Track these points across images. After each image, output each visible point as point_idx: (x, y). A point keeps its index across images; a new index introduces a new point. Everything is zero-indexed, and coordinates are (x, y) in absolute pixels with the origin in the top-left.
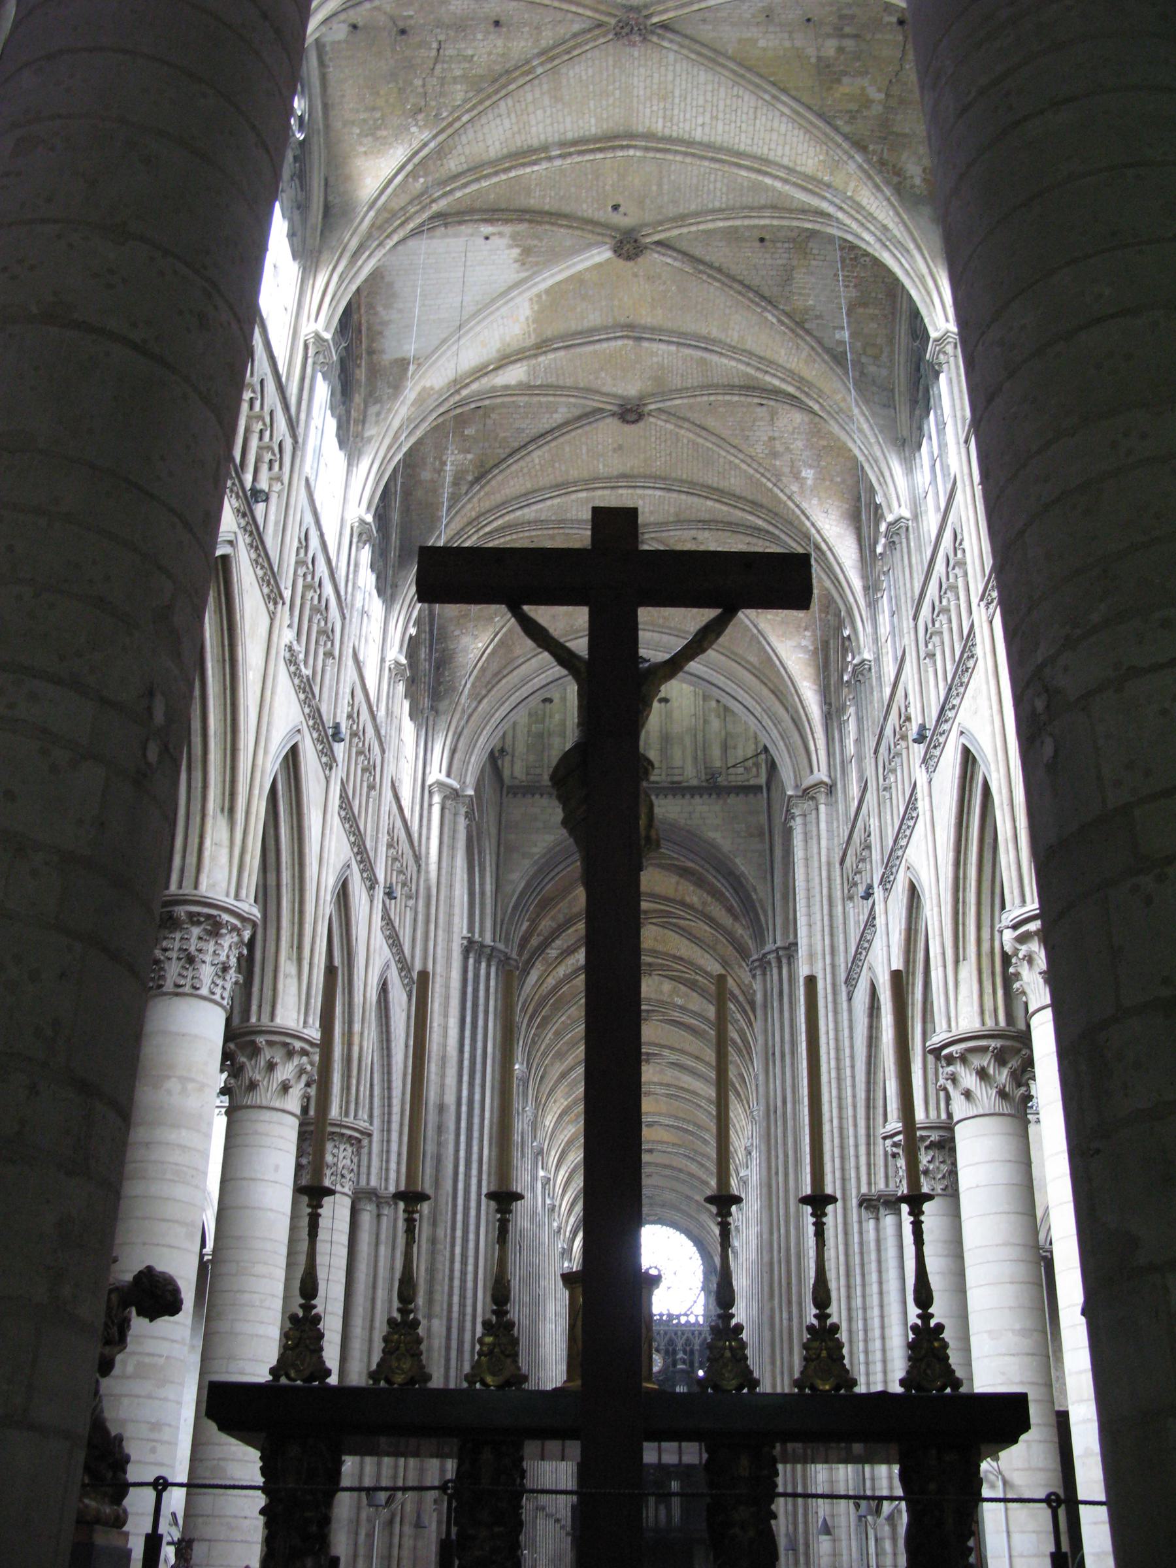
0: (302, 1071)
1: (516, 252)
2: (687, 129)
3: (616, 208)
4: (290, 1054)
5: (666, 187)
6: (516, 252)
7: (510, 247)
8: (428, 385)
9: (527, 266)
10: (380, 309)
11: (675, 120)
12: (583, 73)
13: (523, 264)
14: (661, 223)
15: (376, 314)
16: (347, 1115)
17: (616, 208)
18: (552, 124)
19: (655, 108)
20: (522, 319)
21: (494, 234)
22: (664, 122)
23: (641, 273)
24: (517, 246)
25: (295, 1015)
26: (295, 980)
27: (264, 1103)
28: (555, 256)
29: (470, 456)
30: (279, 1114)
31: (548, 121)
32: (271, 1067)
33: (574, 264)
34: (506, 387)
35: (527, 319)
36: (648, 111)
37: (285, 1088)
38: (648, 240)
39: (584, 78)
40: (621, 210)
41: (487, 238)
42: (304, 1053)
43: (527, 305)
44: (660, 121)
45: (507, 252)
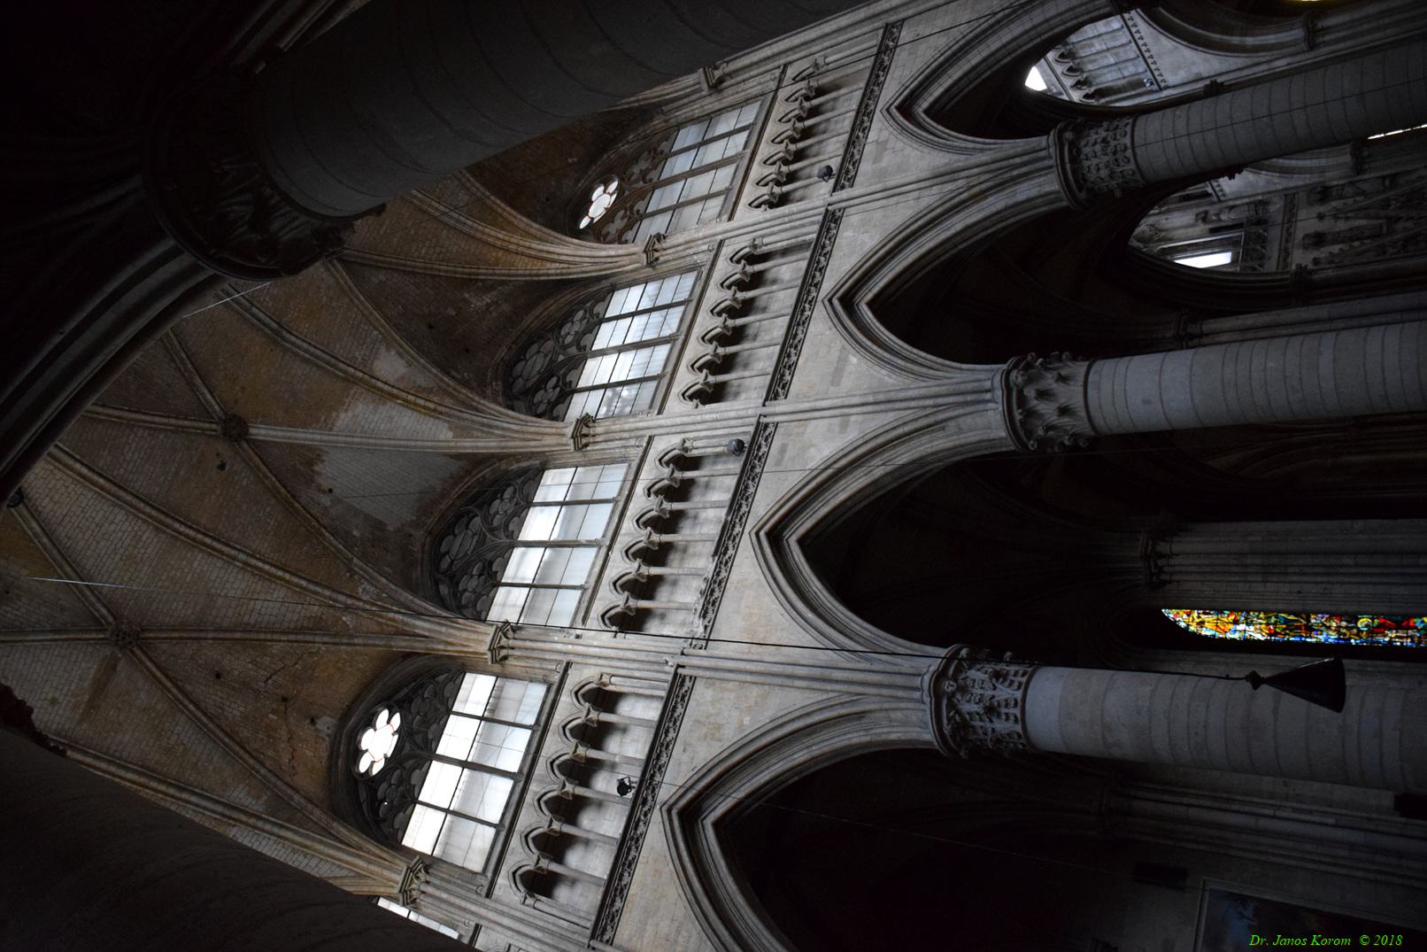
0: (1043, 395)
1: (316, 468)
2: (127, 524)
3: (222, 467)
4: (1030, 414)
5: (173, 469)
6: (316, 468)
7: (319, 473)
8: (450, 435)
9: (318, 452)
10: (439, 490)
11: (133, 533)
12: (180, 607)
13: (319, 455)
14: (197, 434)
15: (444, 489)
16: (1051, 167)
17: (222, 467)
18: (227, 581)
19: (143, 551)
20: (350, 414)
21: (324, 492)
22: (141, 536)
23: (237, 388)
24: (313, 471)
25: (991, 413)
26: (961, 420)
27: (1088, 425)
28: (293, 448)
29: (467, 295)
30: (1091, 410)
31: (228, 585)
32: (1049, 428)
33: (283, 437)
34: (401, 356)
35: (346, 411)
36: (149, 551)
37: (1064, 411)
38: (214, 426)
39: (181, 603)
40: (218, 463)
41: (331, 491)
42: (1022, 400)
43: (339, 423)
44: (144, 538)
45: (324, 471)
